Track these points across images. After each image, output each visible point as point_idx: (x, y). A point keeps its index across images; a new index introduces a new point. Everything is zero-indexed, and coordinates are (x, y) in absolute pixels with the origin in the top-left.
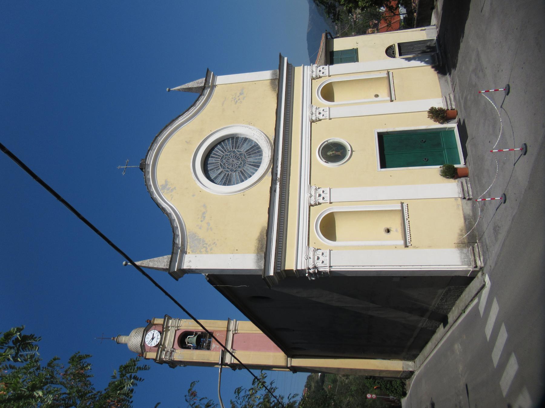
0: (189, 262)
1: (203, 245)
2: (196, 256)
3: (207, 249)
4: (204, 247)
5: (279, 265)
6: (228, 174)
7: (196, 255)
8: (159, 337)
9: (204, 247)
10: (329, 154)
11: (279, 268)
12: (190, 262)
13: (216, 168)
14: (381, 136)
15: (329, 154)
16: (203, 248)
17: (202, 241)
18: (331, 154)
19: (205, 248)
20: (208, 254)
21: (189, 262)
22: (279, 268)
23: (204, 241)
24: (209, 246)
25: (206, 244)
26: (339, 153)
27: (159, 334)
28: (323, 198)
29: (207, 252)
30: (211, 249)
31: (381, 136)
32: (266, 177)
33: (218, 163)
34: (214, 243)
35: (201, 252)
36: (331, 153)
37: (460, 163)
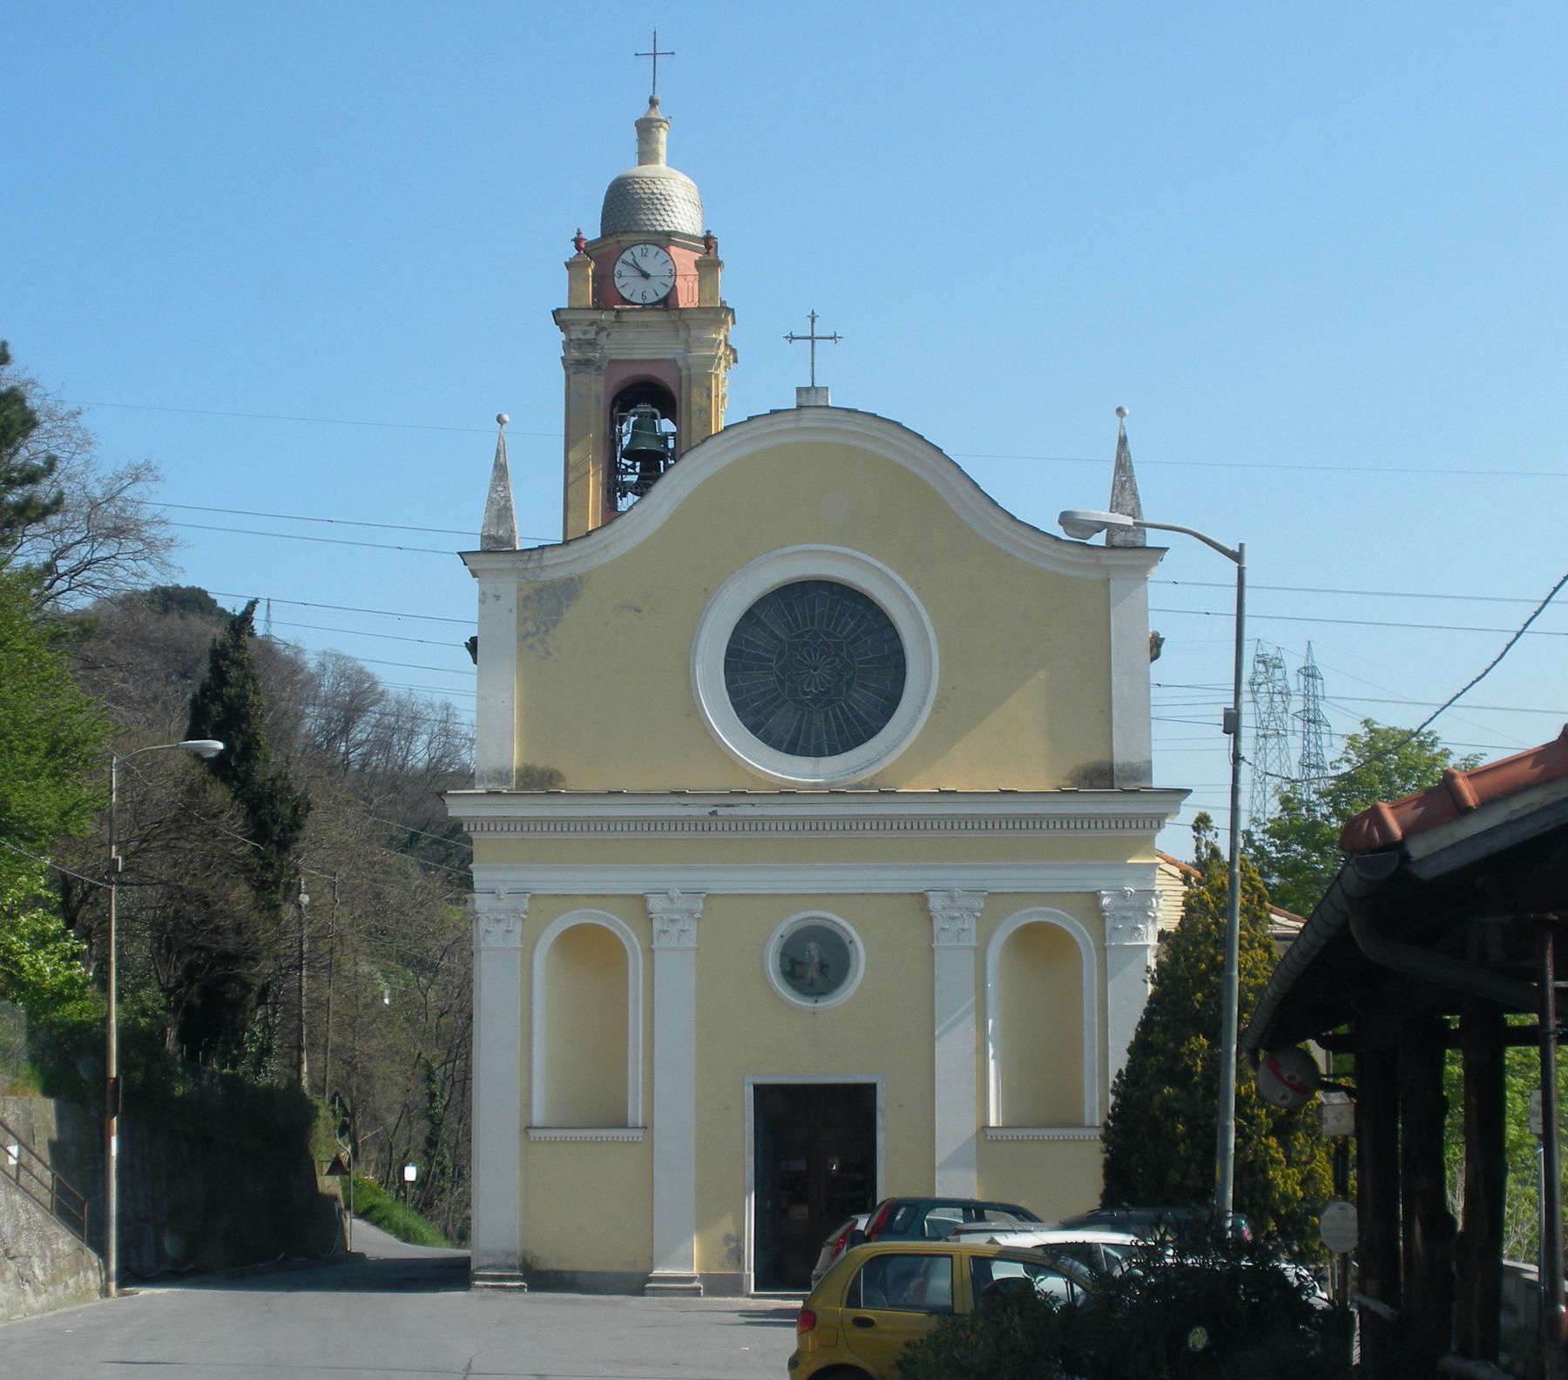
0: (495, 596)
1: (545, 625)
2: (511, 611)
3: (534, 635)
4: (538, 628)
5: (479, 828)
6: (772, 661)
7: (515, 611)
8: (652, 298)
9: (538, 628)
10: (812, 945)
11: (472, 829)
12: (494, 599)
13: (795, 619)
14: (870, 1089)
15: (812, 945)
16: (535, 624)
17: (555, 618)
18: (812, 953)
19: (534, 630)
20: (518, 641)
21: (495, 596)
22: (479, 828)
23: (554, 623)
24: (542, 642)
25: (546, 632)
26: (812, 973)
27: (661, 296)
28: (664, 932)
29: (523, 637)
30: (531, 647)
31: (870, 1089)
32: (1534, 604)
33: (813, 625)
34: (548, 653)
35: (522, 621)
36: (815, 953)
37: (756, 1289)
